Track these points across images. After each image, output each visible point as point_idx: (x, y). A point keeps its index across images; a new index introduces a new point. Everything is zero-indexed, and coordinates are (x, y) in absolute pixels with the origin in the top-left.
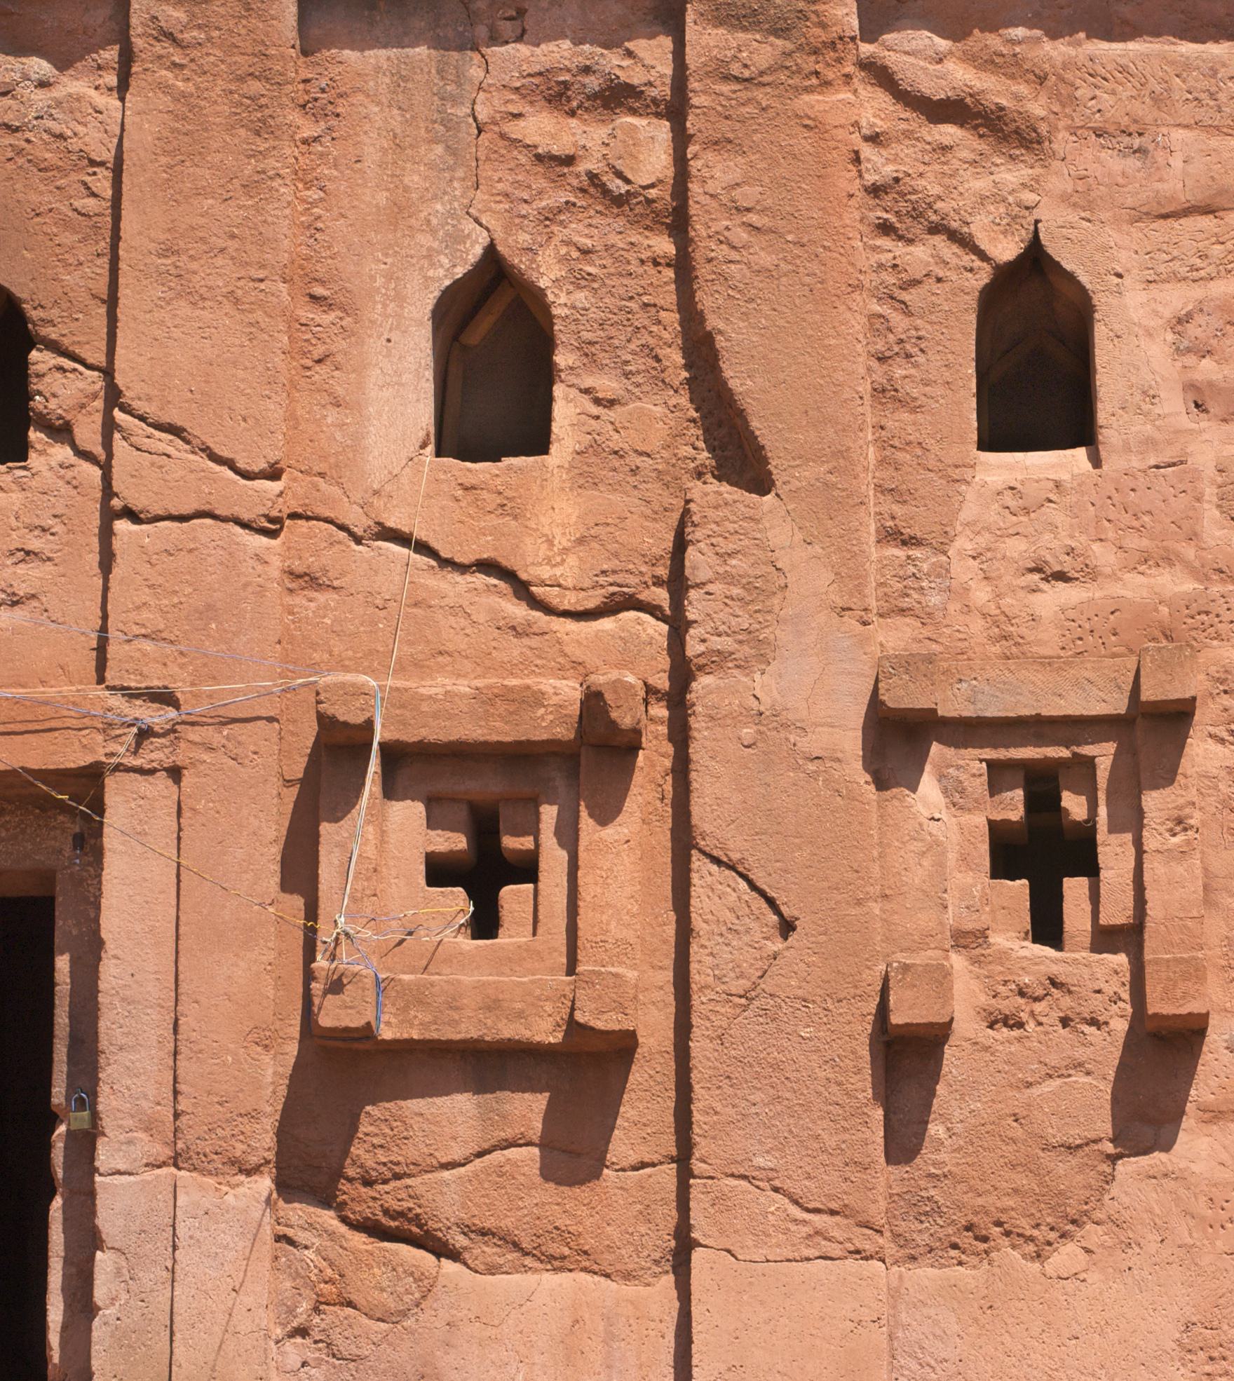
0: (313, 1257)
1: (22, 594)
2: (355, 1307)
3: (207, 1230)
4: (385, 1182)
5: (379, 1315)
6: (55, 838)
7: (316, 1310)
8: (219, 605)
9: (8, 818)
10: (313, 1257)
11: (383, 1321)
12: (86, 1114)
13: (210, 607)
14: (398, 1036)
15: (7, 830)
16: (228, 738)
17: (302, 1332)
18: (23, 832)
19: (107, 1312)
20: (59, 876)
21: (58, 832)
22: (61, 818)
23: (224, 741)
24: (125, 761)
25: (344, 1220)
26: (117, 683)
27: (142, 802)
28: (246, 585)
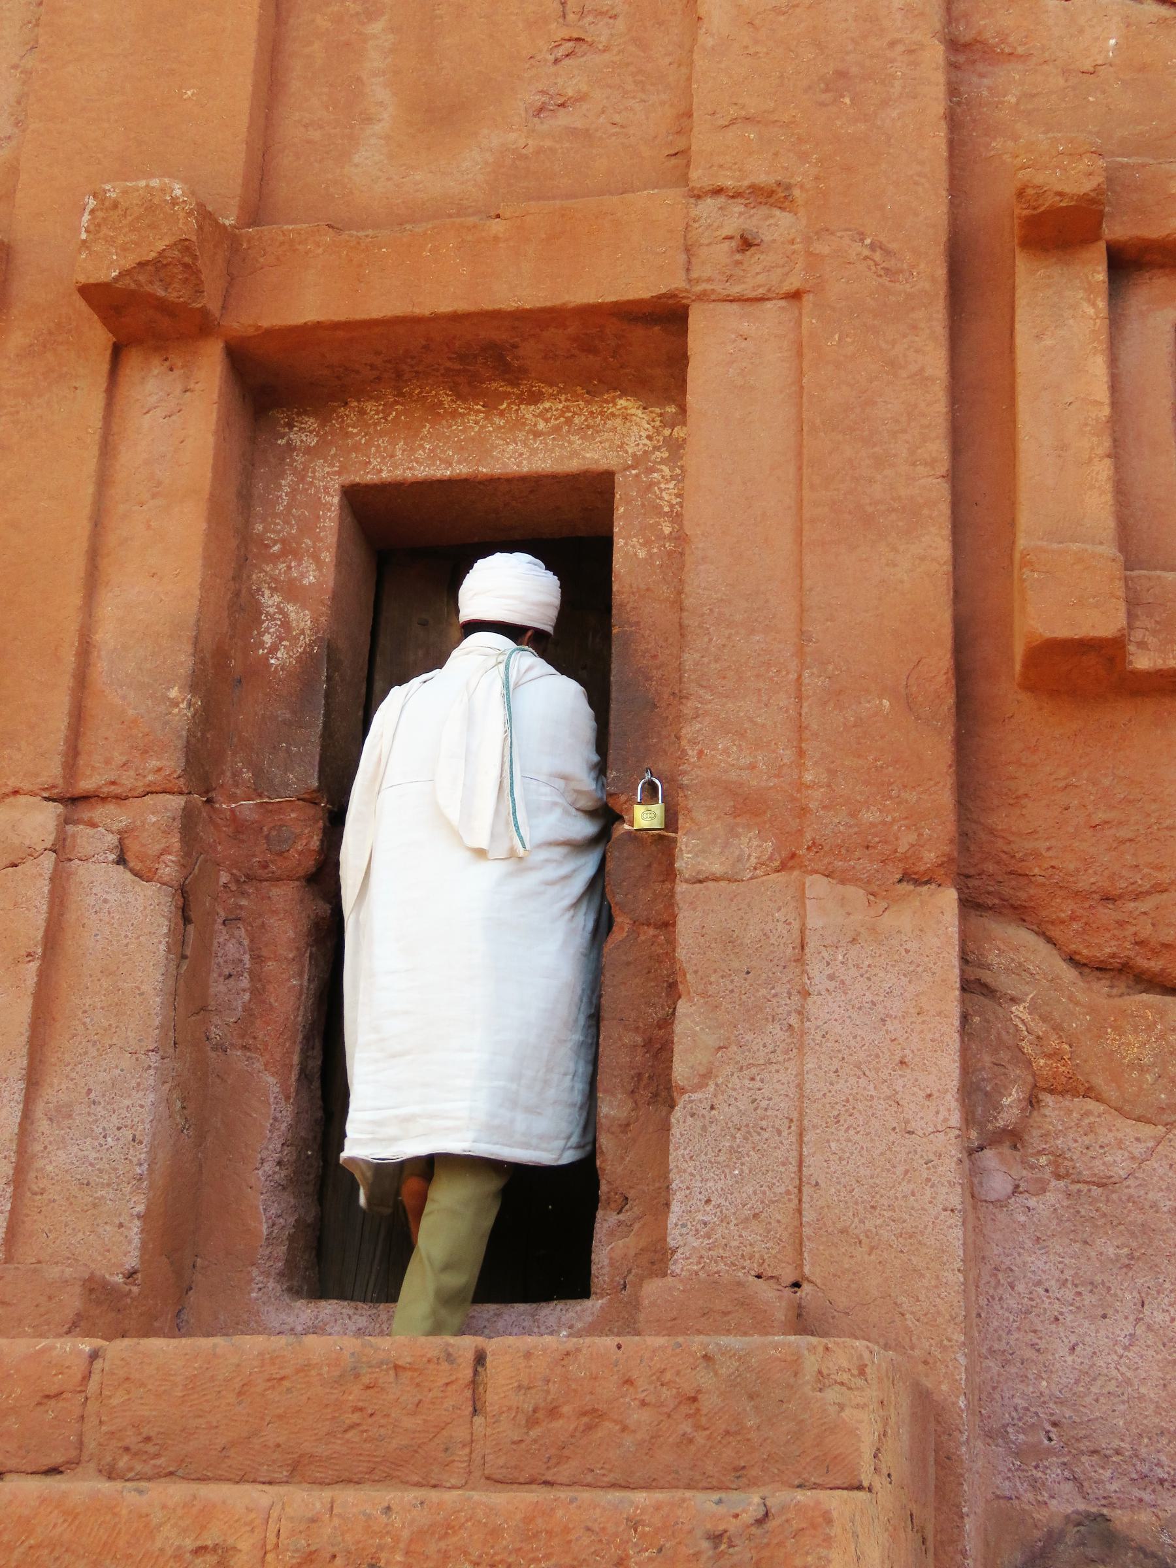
0: (1026, 1016)
1: (570, 93)
2: (1098, 1099)
3: (857, 966)
4: (1138, 896)
5: (1138, 1112)
6: (614, 429)
7: (1033, 1102)
8: (854, 70)
9: (547, 405)
10: (1026, 1016)
11: (1148, 1121)
12: (658, 809)
13: (841, 74)
14: (1160, 664)
15: (547, 421)
16: (872, 247)
17: (1013, 1137)
18: (569, 421)
19: (695, 1096)
20: (619, 478)
21: (619, 421)
22: (622, 402)
23: (866, 252)
24: (718, 288)
25: (1072, 960)
26: (707, 183)
27: (744, 344)
28: (892, 44)
